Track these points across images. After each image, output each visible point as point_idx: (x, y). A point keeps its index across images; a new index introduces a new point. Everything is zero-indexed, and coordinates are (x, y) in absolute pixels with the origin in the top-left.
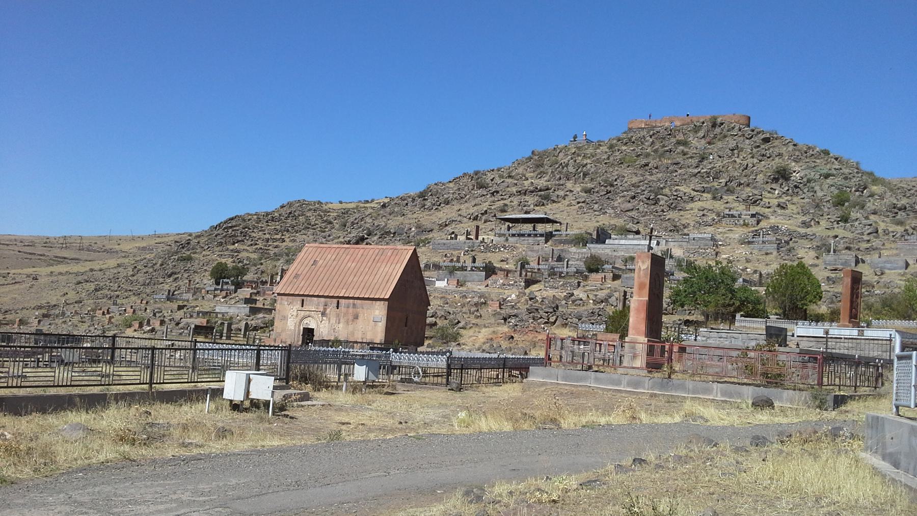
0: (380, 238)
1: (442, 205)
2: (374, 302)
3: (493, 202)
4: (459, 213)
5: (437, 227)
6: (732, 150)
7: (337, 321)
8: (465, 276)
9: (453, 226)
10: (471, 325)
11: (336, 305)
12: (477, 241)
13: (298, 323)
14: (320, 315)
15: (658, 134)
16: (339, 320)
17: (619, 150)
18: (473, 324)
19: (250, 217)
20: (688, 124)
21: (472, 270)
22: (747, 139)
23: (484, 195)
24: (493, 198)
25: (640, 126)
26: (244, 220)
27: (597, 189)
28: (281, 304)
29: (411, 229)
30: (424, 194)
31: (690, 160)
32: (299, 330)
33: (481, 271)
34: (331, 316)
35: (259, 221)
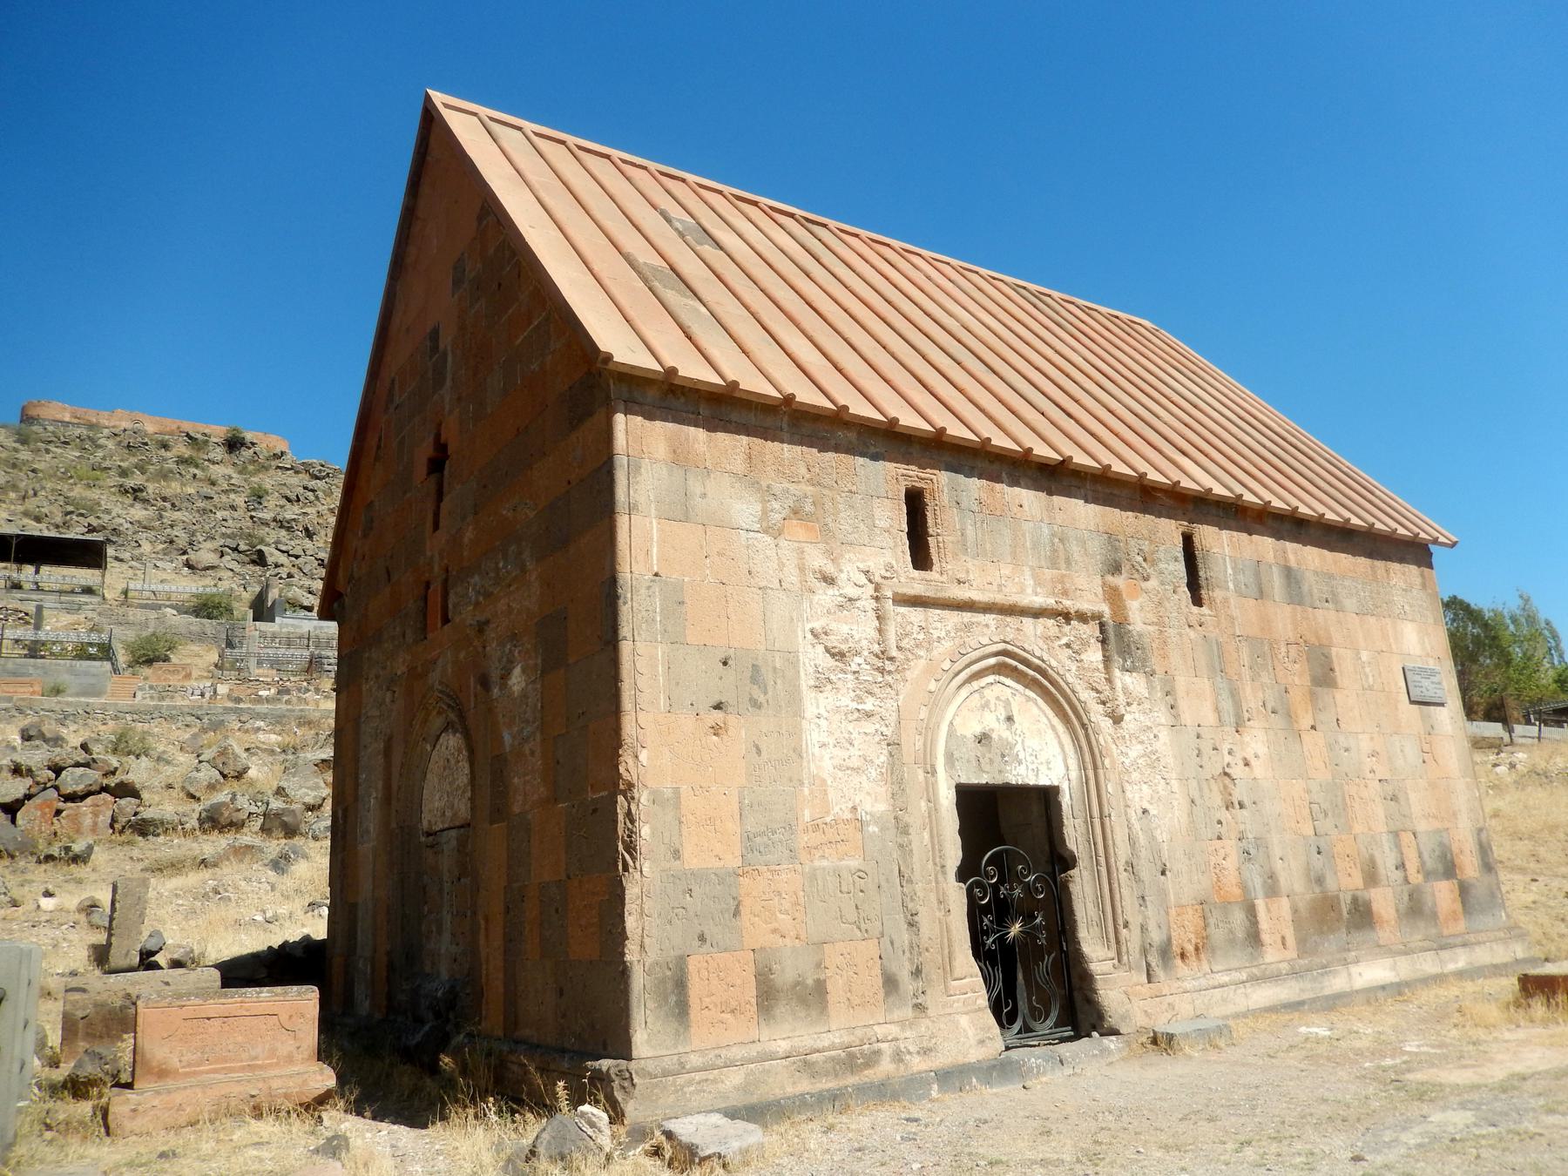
2: (1379, 564)
6: (313, 491)
7: (1227, 705)
11: (1180, 568)
14: (1094, 655)
15: (118, 439)
16: (1234, 694)
17: (48, 451)
20: (171, 433)
22: (317, 478)
25: (59, 417)
27: (59, 519)
28: (680, 511)
31: (232, 496)
33: (91, 658)
34: (1175, 659)
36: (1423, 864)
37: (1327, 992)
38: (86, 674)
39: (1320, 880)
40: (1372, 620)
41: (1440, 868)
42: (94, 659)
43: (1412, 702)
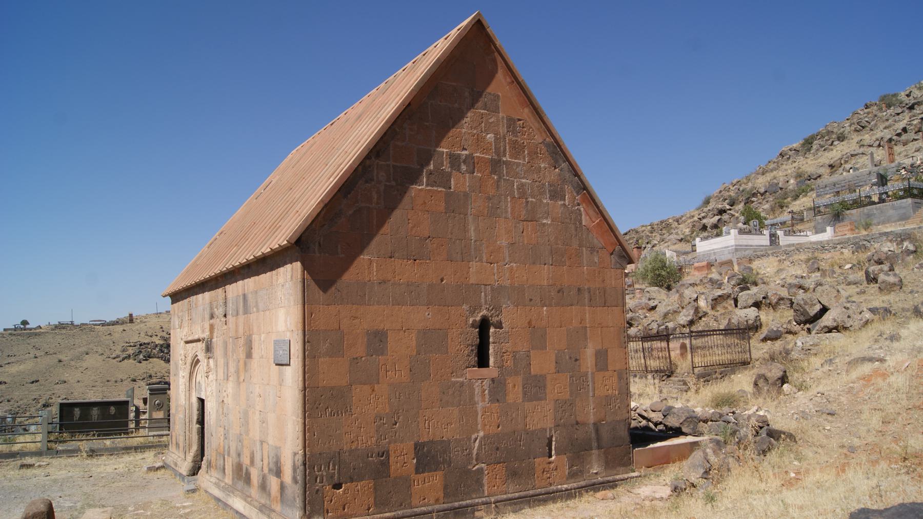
0: (745, 204)
1: (836, 143)
3: (914, 116)
4: (862, 143)
5: (828, 170)
8: (869, 216)
9: (853, 161)
10: (868, 315)
12: (893, 165)
13: (188, 384)
18: (873, 310)
19: (644, 228)
21: (882, 201)
23: (898, 114)
24: (915, 111)
26: (637, 232)
29: (788, 182)
30: (810, 141)
32: (190, 405)
33: (901, 198)
35: (653, 230)
36: (269, 463)
37: (228, 503)
38: (901, 207)
39: (239, 455)
40: (268, 313)
41: (275, 468)
42: (903, 198)
43: (277, 365)
